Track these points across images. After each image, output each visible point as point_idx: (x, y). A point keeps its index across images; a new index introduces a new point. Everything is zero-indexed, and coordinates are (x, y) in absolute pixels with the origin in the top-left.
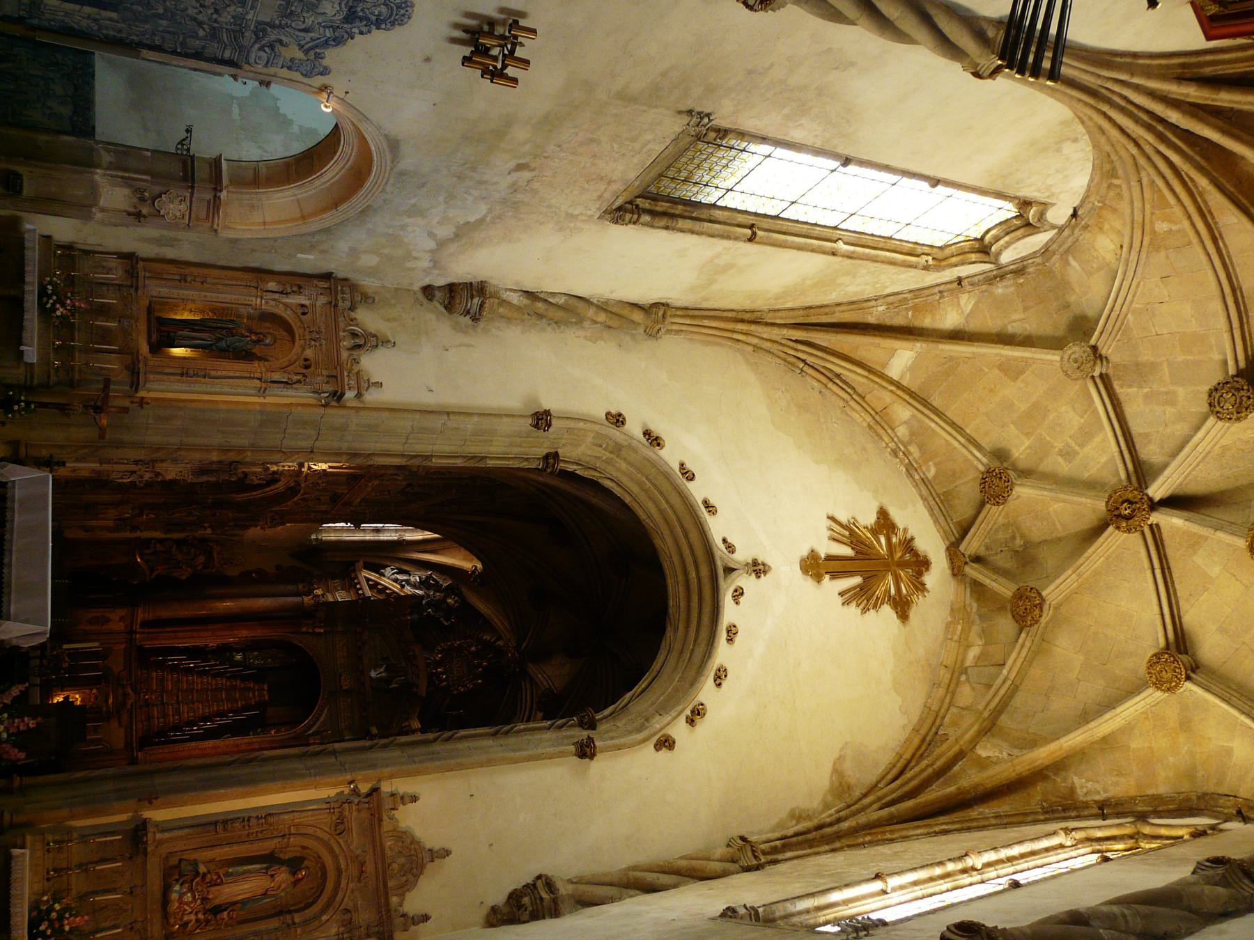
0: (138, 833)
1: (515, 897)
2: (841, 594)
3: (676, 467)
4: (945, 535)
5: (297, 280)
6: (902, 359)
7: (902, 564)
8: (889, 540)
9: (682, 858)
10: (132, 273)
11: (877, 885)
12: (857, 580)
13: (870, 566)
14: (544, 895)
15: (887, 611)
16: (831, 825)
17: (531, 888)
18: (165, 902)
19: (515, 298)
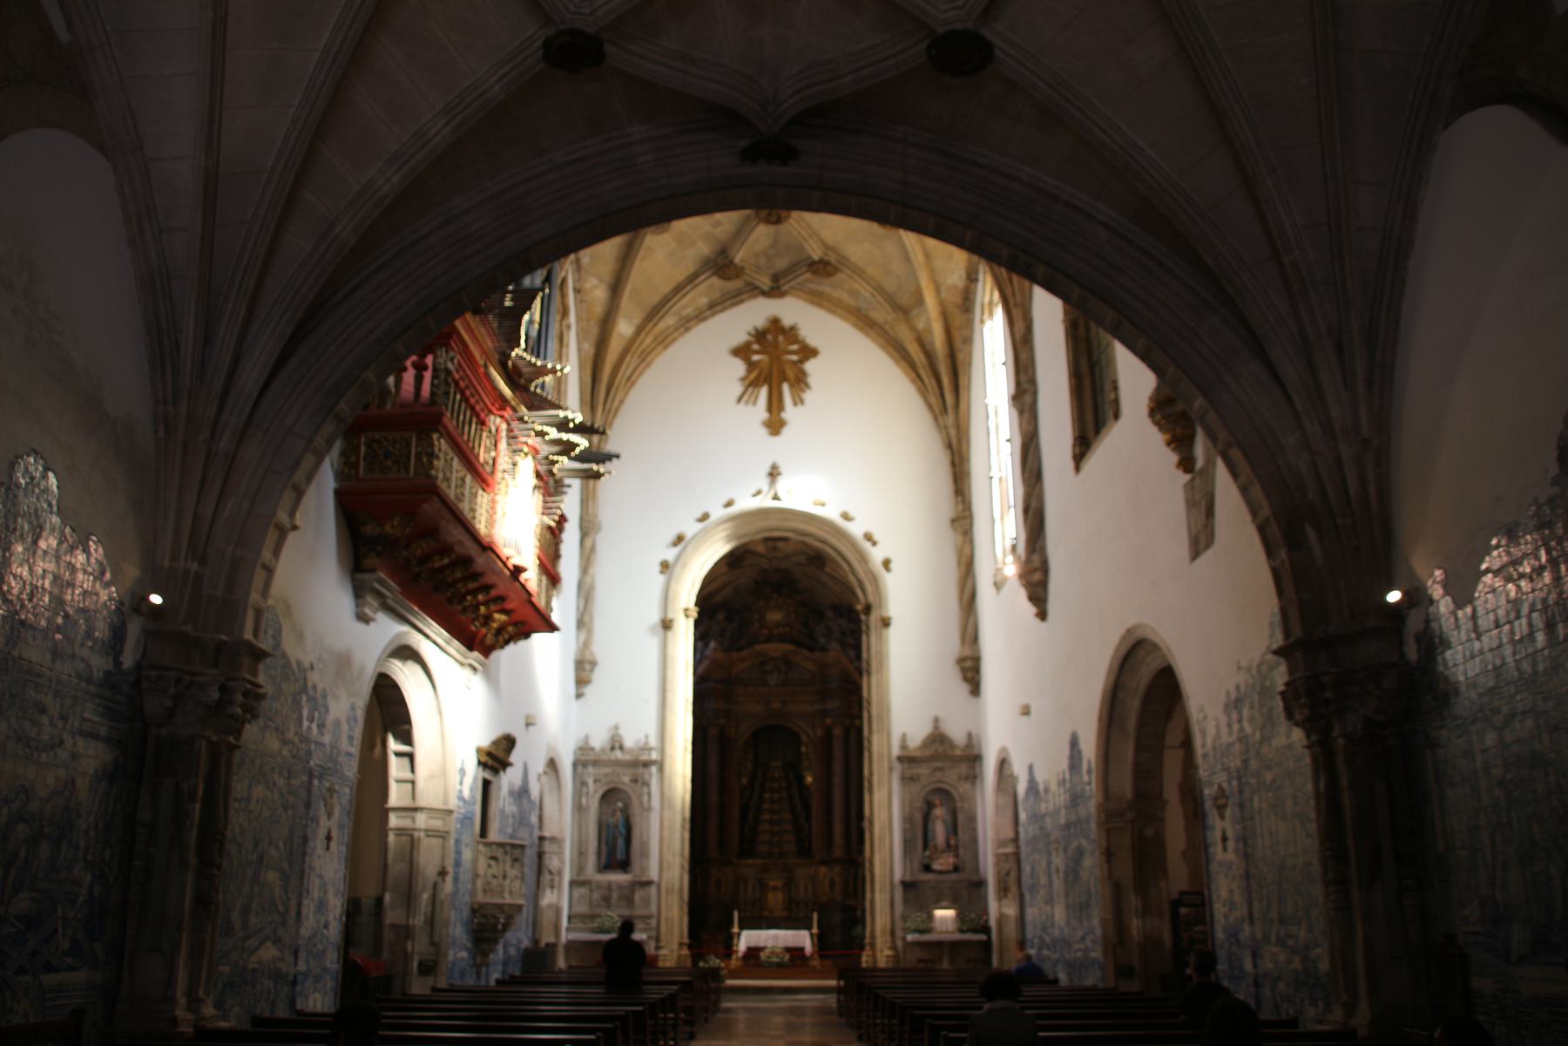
0: (907, 886)
1: (966, 679)
2: (795, 404)
3: (700, 526)
4: (755, 296)
5: (579, 783)
6: (624, 328)
7: (776, 344)
8: (757, 352)
9: (959, 564)
10: (582, 883)
11: (995, 482)
12: (786, 388)
13: (775, 367)
14: (968, 664)
15: (810, 366)
16: (953, 454)
17: (963, 670)
18: (941, 872)
19: (582, 637)
